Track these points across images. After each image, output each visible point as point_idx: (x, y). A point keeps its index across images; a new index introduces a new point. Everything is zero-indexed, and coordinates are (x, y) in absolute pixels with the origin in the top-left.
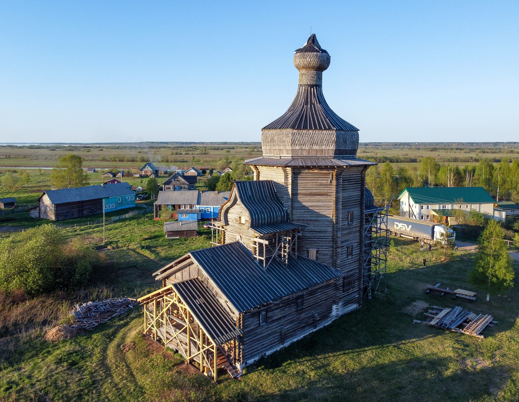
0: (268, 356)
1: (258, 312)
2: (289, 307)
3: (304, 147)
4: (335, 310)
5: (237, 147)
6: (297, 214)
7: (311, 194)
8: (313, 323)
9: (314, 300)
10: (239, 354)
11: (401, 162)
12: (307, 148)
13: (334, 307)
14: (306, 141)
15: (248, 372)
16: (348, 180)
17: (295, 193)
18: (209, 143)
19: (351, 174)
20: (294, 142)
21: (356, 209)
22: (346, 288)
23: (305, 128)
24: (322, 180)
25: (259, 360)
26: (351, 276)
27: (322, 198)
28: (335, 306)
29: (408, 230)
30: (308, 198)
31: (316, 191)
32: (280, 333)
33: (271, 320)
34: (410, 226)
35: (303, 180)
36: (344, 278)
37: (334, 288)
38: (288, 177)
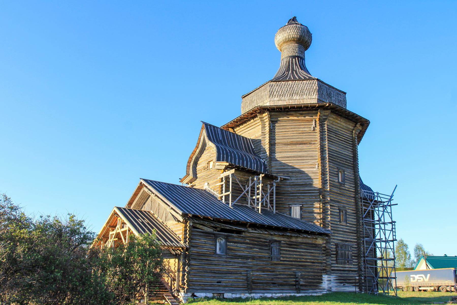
1: (214, 234)
2: (260, 249)
4: (327, 282)
7: (292, 144)
8: (295, 285)
9: (295, 255)
10: (183, 279)
13: (325, 277)
14: (285, 92)
16: (335, 133)
17: (272, 144)
19: (339, 128)
20: (273, 93)
21: (349, 170)
24: (304, 128)
27: (304, 147)
28: (327, 276)
29: (427, 280)
30: (289, 147)
31: (298, 140)
32: (245, 278)
33: (233, 254)
34: (429, 275)
35: (283, 129)
36: (337, 245)
37: (324, 252)
38: (266, 126)
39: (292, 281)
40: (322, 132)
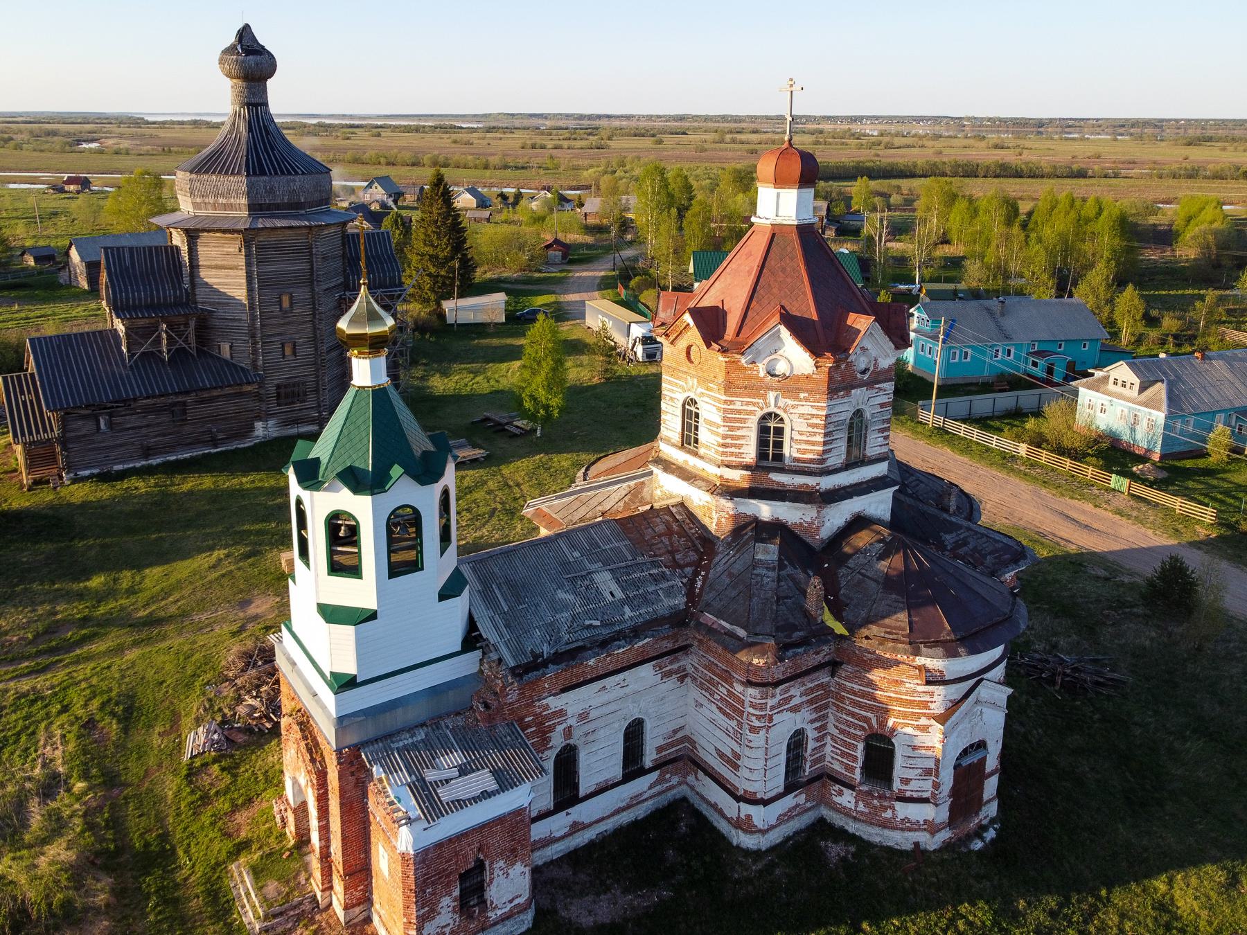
3: (207, 200)
5: (695, 130)
6: (200, 294)
11: (1042, 177)
12: (211, 201)
13: (259, 425)
18: (644, 116)
22: (282, 401)
23: (206, 172)
26: (294, 385)
27: (231, 272)
30: (213, 272)
36: (278, 386)
39: (207, 437)
40: (248, 256)
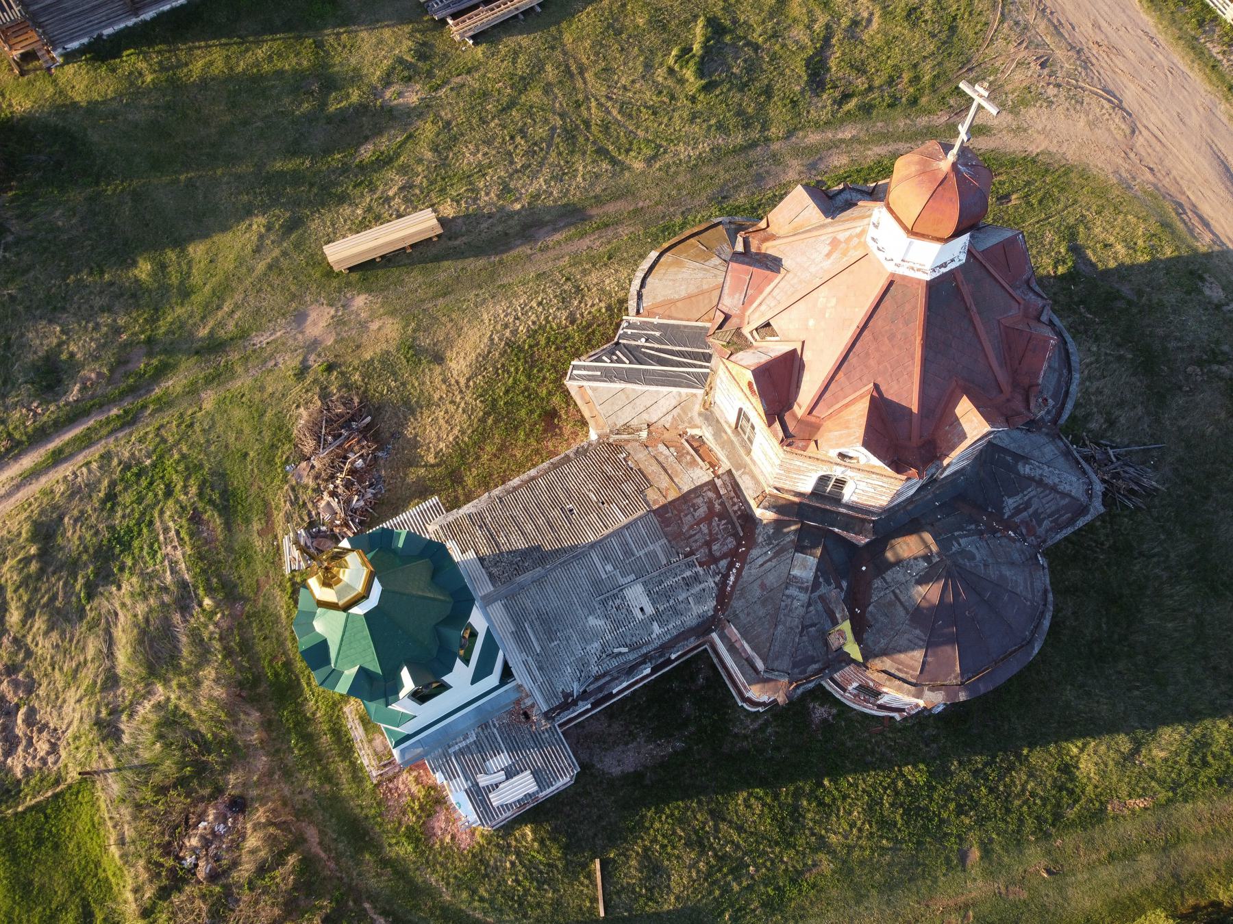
0: (109, 36)
15: (66, 62)
25: (90, 43)
